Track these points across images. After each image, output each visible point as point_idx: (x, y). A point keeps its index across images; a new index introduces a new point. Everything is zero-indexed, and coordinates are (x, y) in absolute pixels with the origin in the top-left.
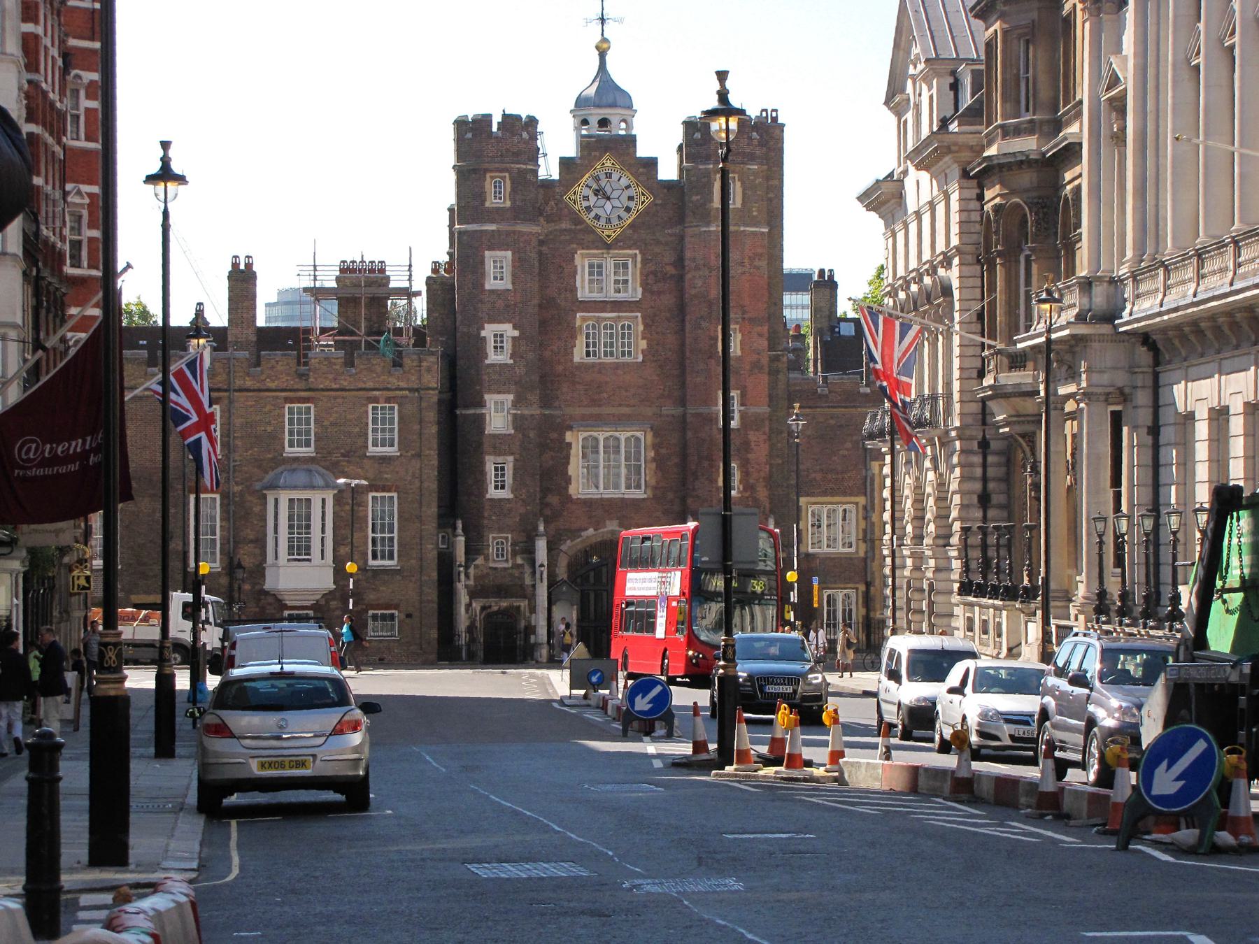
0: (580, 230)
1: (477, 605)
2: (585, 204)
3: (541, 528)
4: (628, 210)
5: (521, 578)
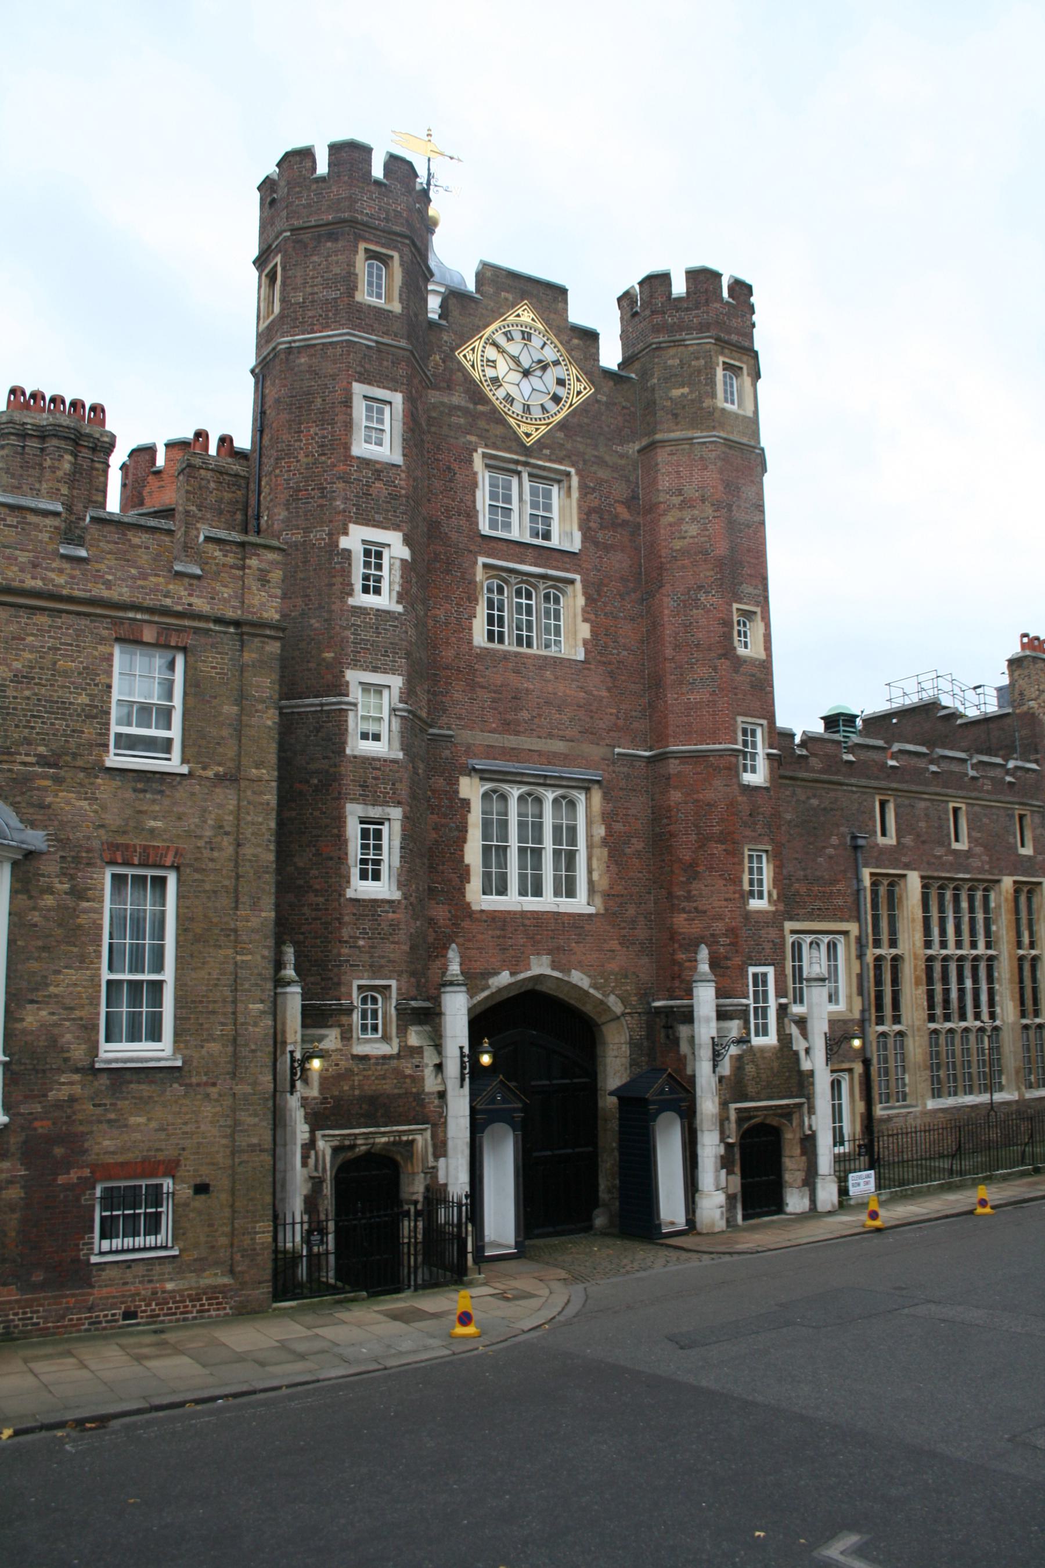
0: (482, 413)
1: (323, 1145)
2: (490, 373)
3: (454, 968)
4: (556, 399)
5: (418, 1080)
